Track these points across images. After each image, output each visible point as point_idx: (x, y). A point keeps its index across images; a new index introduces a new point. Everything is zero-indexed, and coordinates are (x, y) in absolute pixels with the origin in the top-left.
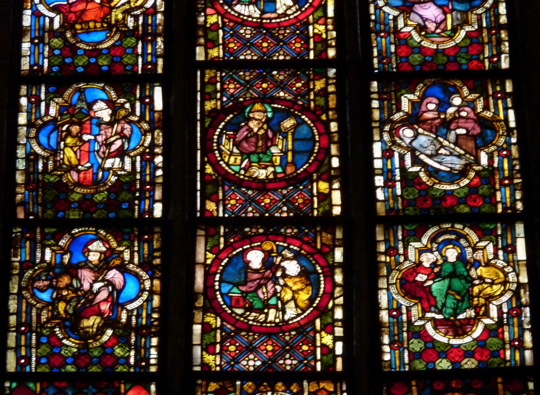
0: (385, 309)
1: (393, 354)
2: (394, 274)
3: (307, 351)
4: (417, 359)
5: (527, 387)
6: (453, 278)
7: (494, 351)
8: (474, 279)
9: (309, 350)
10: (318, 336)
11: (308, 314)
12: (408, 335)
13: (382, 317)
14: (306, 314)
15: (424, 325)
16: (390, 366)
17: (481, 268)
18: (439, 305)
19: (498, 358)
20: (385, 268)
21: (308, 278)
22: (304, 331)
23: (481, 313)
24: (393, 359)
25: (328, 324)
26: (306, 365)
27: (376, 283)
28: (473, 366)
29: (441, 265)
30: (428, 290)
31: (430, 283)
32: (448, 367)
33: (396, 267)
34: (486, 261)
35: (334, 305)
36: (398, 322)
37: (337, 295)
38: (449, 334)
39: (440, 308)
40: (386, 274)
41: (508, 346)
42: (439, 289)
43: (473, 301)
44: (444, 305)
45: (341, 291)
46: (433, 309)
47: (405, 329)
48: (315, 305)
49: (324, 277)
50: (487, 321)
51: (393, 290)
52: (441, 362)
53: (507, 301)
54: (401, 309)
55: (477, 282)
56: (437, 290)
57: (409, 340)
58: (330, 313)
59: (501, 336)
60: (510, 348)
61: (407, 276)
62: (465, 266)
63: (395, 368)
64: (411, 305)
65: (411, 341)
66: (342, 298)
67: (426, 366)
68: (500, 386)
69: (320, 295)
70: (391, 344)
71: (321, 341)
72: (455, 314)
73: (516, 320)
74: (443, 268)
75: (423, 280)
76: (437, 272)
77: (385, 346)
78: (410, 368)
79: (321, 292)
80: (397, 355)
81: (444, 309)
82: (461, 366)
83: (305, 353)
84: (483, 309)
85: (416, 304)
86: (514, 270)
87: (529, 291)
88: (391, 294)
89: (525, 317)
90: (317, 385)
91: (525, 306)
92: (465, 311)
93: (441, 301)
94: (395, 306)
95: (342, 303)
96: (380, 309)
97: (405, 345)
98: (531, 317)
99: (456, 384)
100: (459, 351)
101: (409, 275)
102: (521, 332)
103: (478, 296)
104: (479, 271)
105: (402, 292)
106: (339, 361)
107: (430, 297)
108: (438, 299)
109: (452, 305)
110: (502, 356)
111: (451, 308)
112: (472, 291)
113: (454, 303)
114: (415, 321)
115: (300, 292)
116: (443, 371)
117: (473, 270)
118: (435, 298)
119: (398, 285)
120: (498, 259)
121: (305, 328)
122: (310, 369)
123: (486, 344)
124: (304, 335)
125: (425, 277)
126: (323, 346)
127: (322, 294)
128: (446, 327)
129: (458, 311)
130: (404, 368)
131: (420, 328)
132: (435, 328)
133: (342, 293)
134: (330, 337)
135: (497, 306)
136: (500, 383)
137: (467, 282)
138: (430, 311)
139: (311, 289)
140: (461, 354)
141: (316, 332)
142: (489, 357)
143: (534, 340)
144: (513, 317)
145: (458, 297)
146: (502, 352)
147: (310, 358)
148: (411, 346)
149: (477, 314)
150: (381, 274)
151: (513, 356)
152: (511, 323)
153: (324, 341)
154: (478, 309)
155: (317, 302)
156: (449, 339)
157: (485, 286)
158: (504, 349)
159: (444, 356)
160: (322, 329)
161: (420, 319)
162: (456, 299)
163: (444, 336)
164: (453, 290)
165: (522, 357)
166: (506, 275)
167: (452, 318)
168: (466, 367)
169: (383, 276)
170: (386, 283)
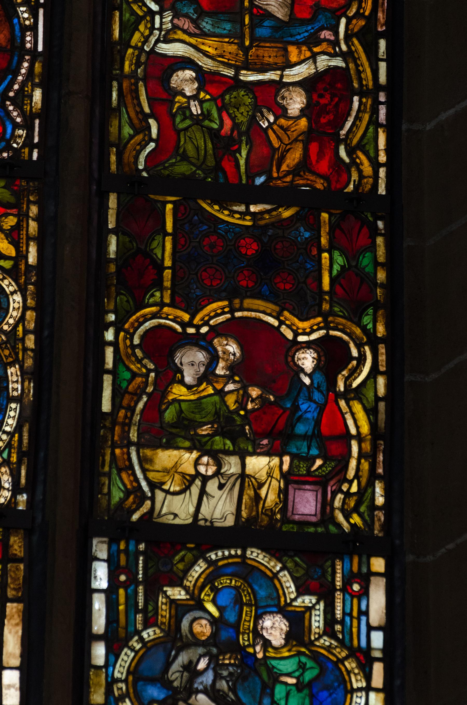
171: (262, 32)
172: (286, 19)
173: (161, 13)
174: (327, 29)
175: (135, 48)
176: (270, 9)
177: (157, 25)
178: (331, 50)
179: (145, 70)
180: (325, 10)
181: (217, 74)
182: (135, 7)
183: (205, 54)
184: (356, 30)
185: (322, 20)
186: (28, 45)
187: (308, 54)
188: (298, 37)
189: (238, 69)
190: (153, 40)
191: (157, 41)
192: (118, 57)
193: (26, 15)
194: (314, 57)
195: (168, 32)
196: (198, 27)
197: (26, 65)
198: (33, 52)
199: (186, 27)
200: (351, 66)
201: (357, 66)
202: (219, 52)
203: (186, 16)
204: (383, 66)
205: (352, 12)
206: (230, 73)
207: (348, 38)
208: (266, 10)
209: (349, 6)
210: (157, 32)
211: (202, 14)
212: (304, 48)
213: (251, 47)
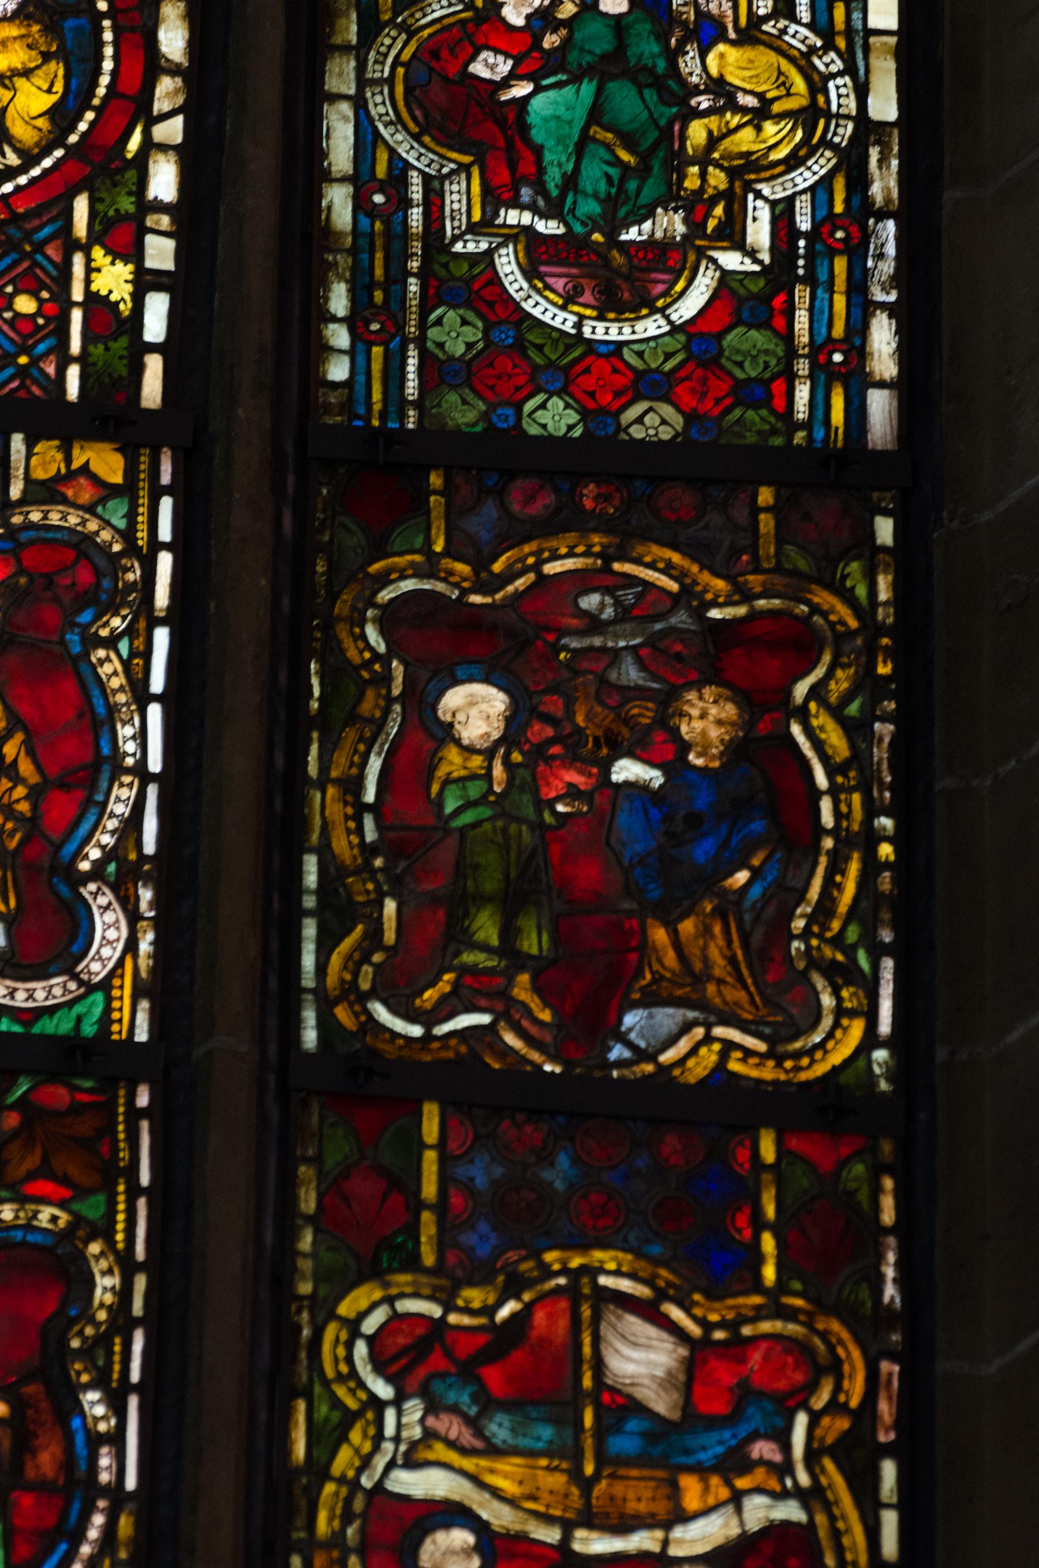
0: (343, 180)
1: (361, 360)
2: (387, 41)
3: (33, 317)
4: (454, 387)
5: (871, 533)
6: (615, 77)
7: (749, 380)
8: (696, 91)
9: (39, 313)
10: (78, 261)
11: (45, 172)
12: (423, 288)
13: (329, 208)
14: (36, 172)
15: (489, 253)
16: (347, 407)
17: (721, 47)
18: (553, 178)
19: (764, 412)
20: (354, 16)
21: (51, 29)
22: (28, 236)
23: (711, 224)
24: (361, 378)
25: (121, 217)
26: (23, 372)
27: (318, 75)
28: (666, 434)
29: (570, 23)
30: (512, 117)
31: (521, 89)
32: (570, 428)
33: (396, 14)
34: (743, 21)
35: (149, 145)
36: (387, 232)
37: (161, 105)
38: (581, 300)
39: (555, 193)
40: (354, 39)
41: (803, 367)
42: (558, 118)
43: (682, 177)
44: (571, 182)
45: (177, 91)
46: (526, 194)
47: (414, 264)
48: (73, 139)
49: (115, 29)
50: (731, 260)
51: (379, 106)
52: (543, 406)
53: (812, 189)
54: (405, 183)
55: (704, 102)
56: (545, 120)
57: (425, 310)
58: (131, 175)
59: (779, 322)
60: (811, 376)
61: (435, 55)
62: (662, 38)
63: (368, 419)
64: (445, 170)
65: (433, 316)
66: (179, 121)
67: (485, 416)
68: (766, 523)
69: (96, 102)
70: (354, 322)
71: (88, 282)
72: (613, 227)
73: (840, 265)
74: (578, 36)
75: (497, 78)
76: (554, 50)
77: (332, 327)
78: (420, 422)
79: (101, 91)
80: (377, 366)
81: (569, 200)
82: (619, 428)
83: (27, 328)
84: (719, 211)
85: (466, 168)
86: (850, 69)
87: (900, 156)
88: (371, 121)
89: (880, 256)
90: (59, 456)
91: (881, 215)
92: (651, 214)
93: (560, 165)
94: (381, 170)
95: (179, 140)
96: (327, 177)
97: (412, 330)
98: (897, 258)
99: (597, 498)
100: (615, 370)
101: (445, 53)
102: (857, 313)
103: (704, 160)
104: (712, 60)
105: (414, 119)
106: (154, 365)
107: (519, 144)
108: (548, 157)
109: (603, 186)
110: (779, 404)
111: (596, 196)
112: (683, 138)
113: (609, 179)
114: (455, 239)
115: (20, 83)
116: (548, 441)
117: (692, 52)
118: (538, 151)
119: (400, 89)
120: (794, 19)
121: (28, 226)
122: (36, 391)
123: (721, 351)
124: (26, 255)
125: (505, 67)
126: (96, 303)
127: (105, 98)
128: (574, 271)
129: (622, 212)
130: (402, 416)
131: (472, 267)
132: (530, 273)
133: (180, 100)
134: (124, 271)
135: (773, 204)
136: (767, 509)
137: (666, 97)
138: (516, 203)
139: (61, 73)
140: (620, 381)
141: (72, 246)
142: (728, 401)
143: (904, 353)
144: (832, 253)
145: (625, 156)
146: (778, 387)
147: (41, 348)
148: (433, 333)
149: (695, 225)
150: (338, 40)
151: (820, 404)
152: (823, 276)
153: (101, 284)
154: (700, 210)
155: (83, 126)
156: (581, 318)
157: (735, 120)
158: (790, 378)
159: (558, 385)
160: (95, 237)
161: (474, 229)
162: (618, 162)
163: (563, 308)
164: (607, 128)
165: (857, 412)
166: (817, 84)
167: (597, 237)
168: (637, 433)
169: (346, 48)
170: (352, 75)
171: (622, 1444)
172: (675, 1416)
173: (398, 1402)
174: (768, 1437)
175: (342, 1480)
176: (639, 1394)
177: (390, 1430)
178: (774, 1485)
179: (362, 1531)
180: (761, 1395)
181: (522, 1538)
182: (341, 1391)
183: (496, 1493)
184: (830, 1440)
185: (754, 1418)
186: (104, 1477)
187: (724, 1493)
188: (702, 1456)
189: (568, 1528)
190: (380, 1463)
191: (391, 1465)
192: (303, 1503)
193: (100, 1410)
194: (737, 1499)
195: (414, 1445)
196: (479, 1433)
197: (98, 1520)
198: (116, 1491)
199: (453, 1434)
200: (821, 1519)
201: (832, 1519)
202: (526, 1489)
203: (454, 1409)
204: (890, 1520)
205: (820, 1400)
206: (551, 1535)
207: (812, 1457)
208: (630, 1397)
209: (813, 1387)
210: (388, 1447)
211: (488, 1404)
212: (715, 1480)
213: (597, 1476)
